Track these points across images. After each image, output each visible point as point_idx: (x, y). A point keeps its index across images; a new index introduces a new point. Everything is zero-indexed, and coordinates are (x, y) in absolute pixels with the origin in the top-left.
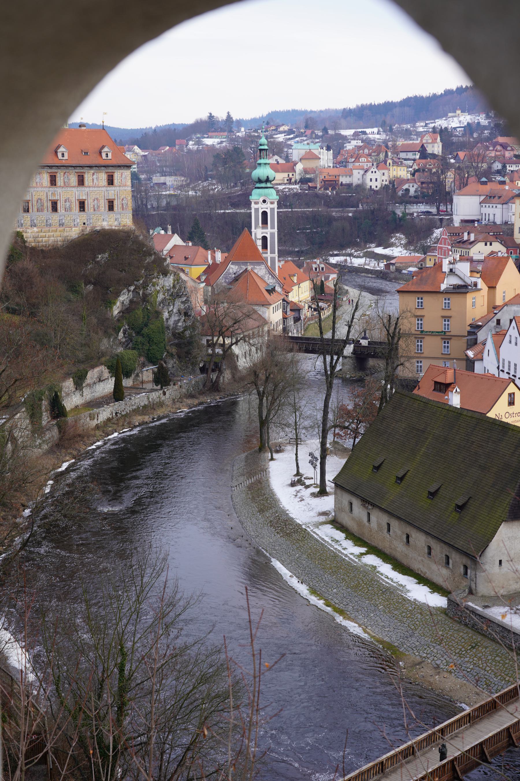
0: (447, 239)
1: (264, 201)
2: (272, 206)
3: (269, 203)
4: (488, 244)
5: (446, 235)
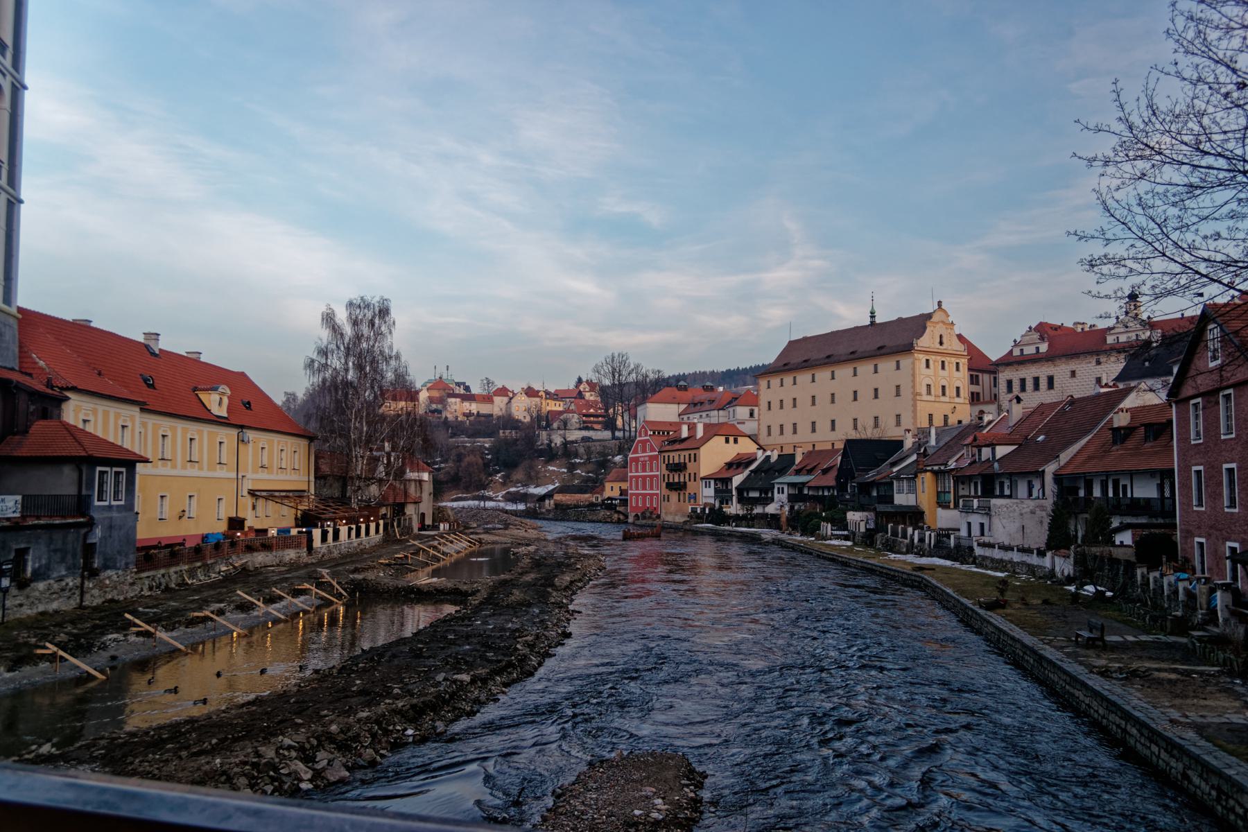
0: (648, 441)
4: (731, 439)
5: (646, 435)
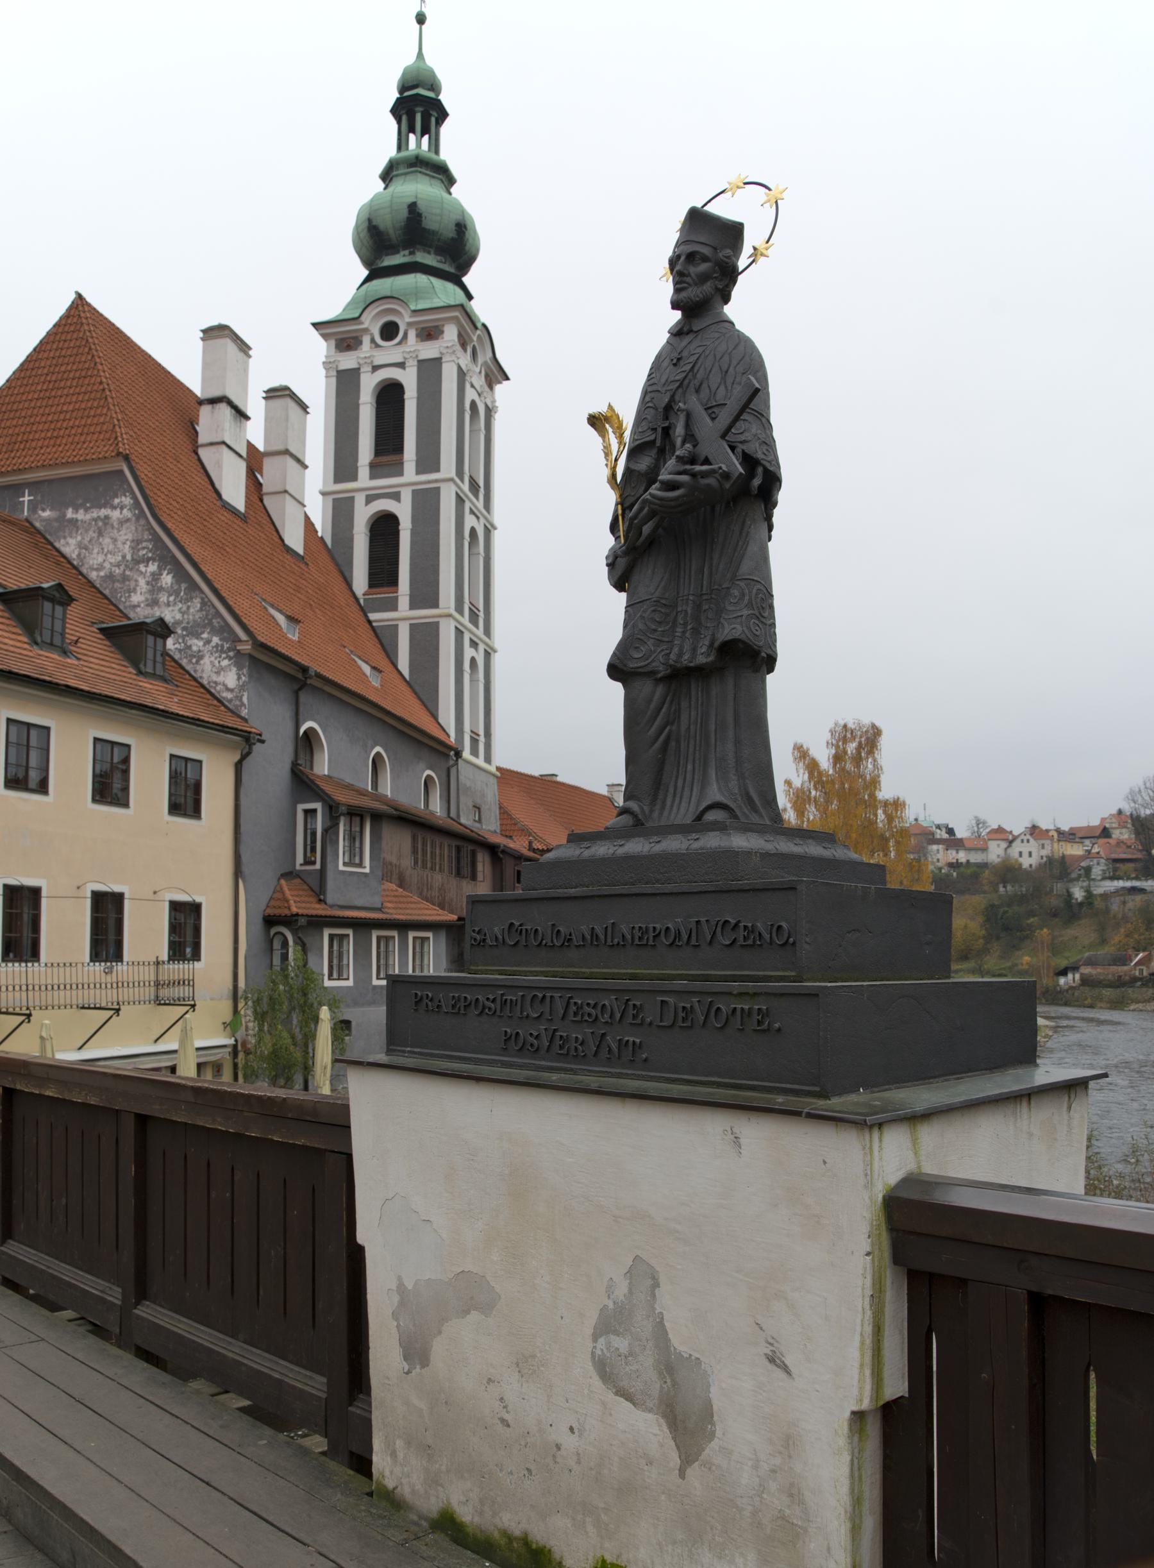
1: (389, 331)
2: (429, 350)
3: (412, 334)
